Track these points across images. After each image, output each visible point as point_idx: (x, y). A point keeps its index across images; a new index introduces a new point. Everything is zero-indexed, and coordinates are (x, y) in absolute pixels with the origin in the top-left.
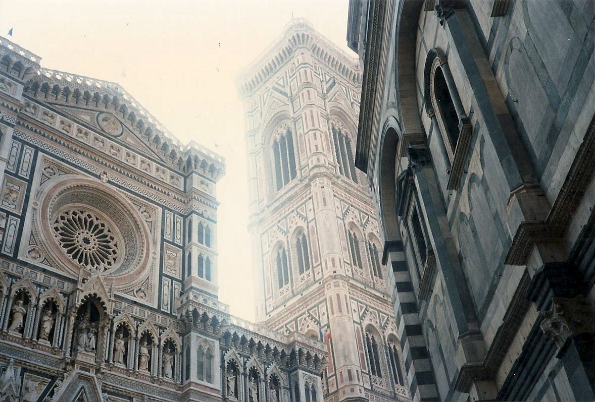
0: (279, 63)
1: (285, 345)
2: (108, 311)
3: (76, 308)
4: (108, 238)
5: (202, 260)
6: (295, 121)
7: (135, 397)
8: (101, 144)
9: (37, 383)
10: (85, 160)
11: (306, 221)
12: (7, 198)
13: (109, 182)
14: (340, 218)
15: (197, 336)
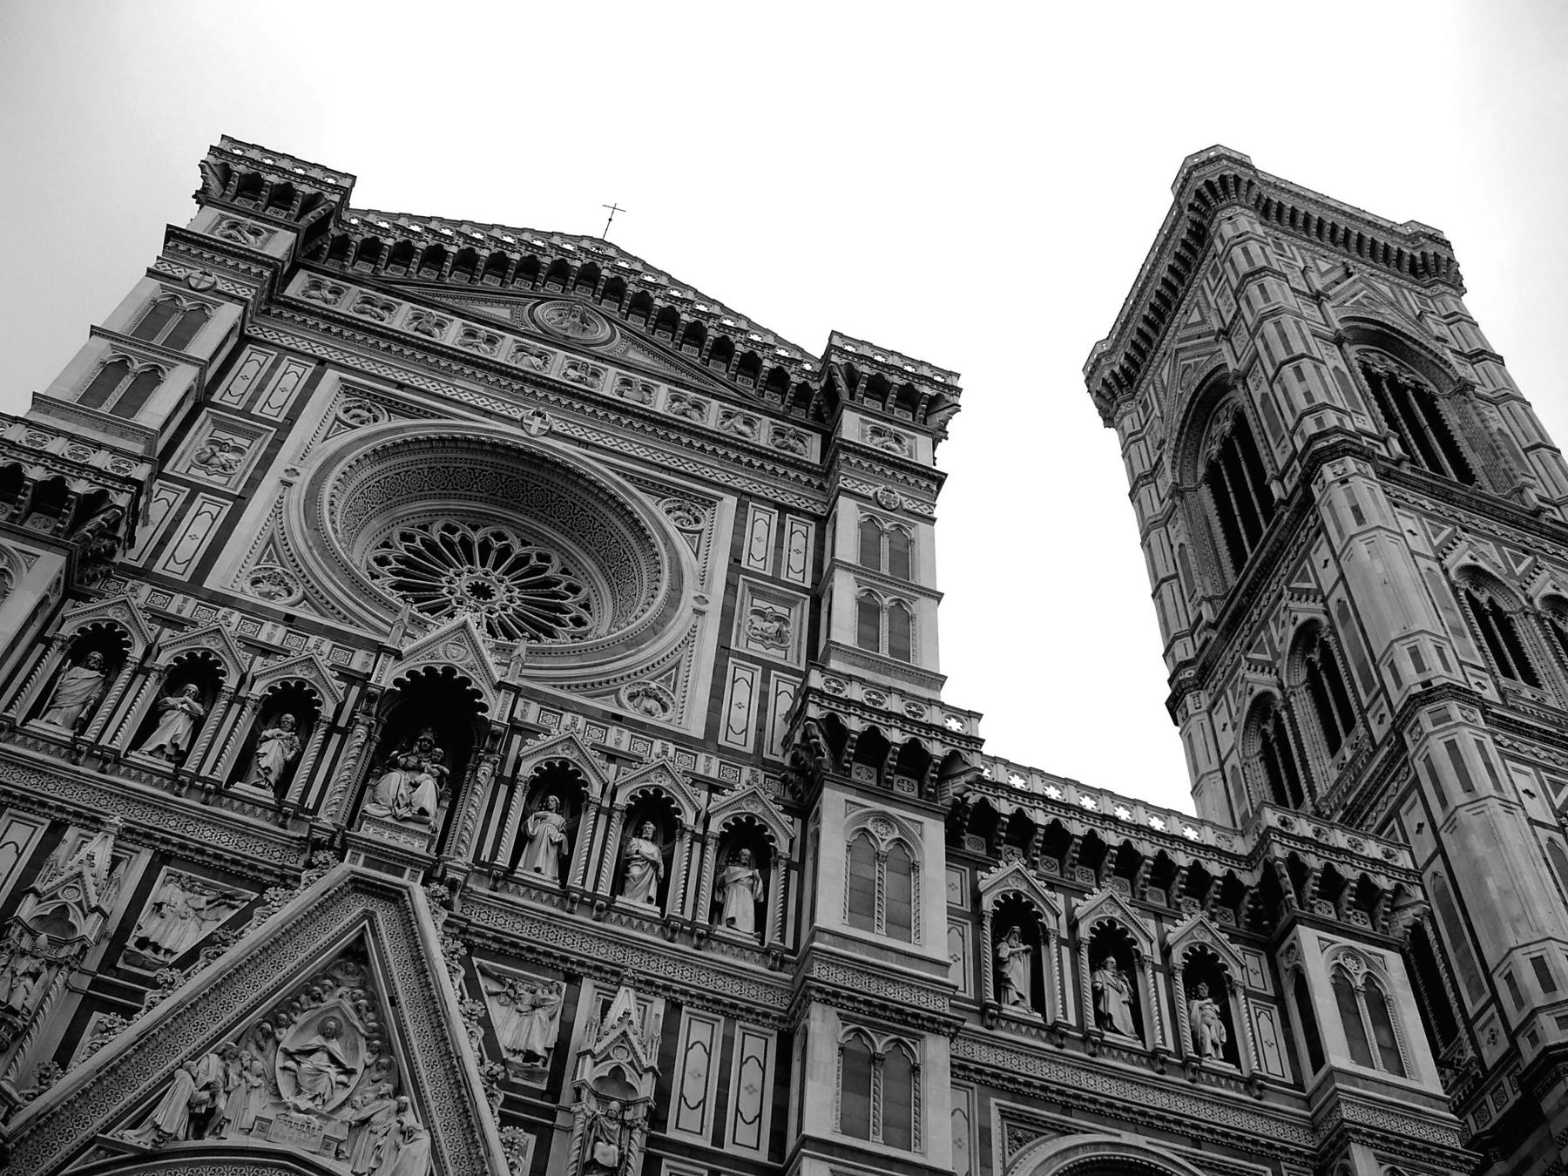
0: (1181, 279)
1: (1234, 857)
2: (492, 715)
3: (371, 698)
4: (561, 588)
5: (877, 610)
6: (1243, 377)
7: (590, 976)
8: (540, 363)
9: (204, 899)
10: (481, 390)
11: (1319, 598)
12: (205, 462)
13: (551, 433)
14: (1427, 557)
15: (847, 801)
